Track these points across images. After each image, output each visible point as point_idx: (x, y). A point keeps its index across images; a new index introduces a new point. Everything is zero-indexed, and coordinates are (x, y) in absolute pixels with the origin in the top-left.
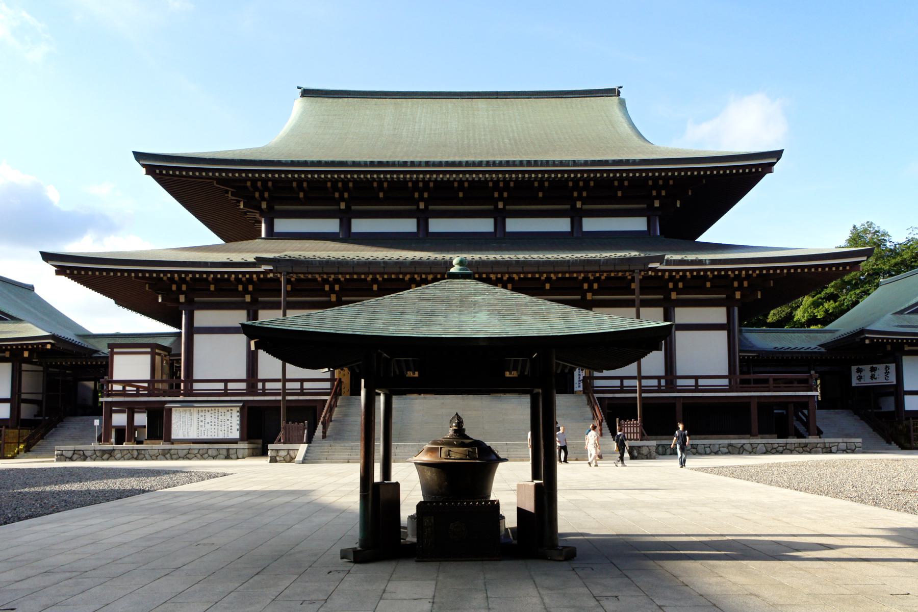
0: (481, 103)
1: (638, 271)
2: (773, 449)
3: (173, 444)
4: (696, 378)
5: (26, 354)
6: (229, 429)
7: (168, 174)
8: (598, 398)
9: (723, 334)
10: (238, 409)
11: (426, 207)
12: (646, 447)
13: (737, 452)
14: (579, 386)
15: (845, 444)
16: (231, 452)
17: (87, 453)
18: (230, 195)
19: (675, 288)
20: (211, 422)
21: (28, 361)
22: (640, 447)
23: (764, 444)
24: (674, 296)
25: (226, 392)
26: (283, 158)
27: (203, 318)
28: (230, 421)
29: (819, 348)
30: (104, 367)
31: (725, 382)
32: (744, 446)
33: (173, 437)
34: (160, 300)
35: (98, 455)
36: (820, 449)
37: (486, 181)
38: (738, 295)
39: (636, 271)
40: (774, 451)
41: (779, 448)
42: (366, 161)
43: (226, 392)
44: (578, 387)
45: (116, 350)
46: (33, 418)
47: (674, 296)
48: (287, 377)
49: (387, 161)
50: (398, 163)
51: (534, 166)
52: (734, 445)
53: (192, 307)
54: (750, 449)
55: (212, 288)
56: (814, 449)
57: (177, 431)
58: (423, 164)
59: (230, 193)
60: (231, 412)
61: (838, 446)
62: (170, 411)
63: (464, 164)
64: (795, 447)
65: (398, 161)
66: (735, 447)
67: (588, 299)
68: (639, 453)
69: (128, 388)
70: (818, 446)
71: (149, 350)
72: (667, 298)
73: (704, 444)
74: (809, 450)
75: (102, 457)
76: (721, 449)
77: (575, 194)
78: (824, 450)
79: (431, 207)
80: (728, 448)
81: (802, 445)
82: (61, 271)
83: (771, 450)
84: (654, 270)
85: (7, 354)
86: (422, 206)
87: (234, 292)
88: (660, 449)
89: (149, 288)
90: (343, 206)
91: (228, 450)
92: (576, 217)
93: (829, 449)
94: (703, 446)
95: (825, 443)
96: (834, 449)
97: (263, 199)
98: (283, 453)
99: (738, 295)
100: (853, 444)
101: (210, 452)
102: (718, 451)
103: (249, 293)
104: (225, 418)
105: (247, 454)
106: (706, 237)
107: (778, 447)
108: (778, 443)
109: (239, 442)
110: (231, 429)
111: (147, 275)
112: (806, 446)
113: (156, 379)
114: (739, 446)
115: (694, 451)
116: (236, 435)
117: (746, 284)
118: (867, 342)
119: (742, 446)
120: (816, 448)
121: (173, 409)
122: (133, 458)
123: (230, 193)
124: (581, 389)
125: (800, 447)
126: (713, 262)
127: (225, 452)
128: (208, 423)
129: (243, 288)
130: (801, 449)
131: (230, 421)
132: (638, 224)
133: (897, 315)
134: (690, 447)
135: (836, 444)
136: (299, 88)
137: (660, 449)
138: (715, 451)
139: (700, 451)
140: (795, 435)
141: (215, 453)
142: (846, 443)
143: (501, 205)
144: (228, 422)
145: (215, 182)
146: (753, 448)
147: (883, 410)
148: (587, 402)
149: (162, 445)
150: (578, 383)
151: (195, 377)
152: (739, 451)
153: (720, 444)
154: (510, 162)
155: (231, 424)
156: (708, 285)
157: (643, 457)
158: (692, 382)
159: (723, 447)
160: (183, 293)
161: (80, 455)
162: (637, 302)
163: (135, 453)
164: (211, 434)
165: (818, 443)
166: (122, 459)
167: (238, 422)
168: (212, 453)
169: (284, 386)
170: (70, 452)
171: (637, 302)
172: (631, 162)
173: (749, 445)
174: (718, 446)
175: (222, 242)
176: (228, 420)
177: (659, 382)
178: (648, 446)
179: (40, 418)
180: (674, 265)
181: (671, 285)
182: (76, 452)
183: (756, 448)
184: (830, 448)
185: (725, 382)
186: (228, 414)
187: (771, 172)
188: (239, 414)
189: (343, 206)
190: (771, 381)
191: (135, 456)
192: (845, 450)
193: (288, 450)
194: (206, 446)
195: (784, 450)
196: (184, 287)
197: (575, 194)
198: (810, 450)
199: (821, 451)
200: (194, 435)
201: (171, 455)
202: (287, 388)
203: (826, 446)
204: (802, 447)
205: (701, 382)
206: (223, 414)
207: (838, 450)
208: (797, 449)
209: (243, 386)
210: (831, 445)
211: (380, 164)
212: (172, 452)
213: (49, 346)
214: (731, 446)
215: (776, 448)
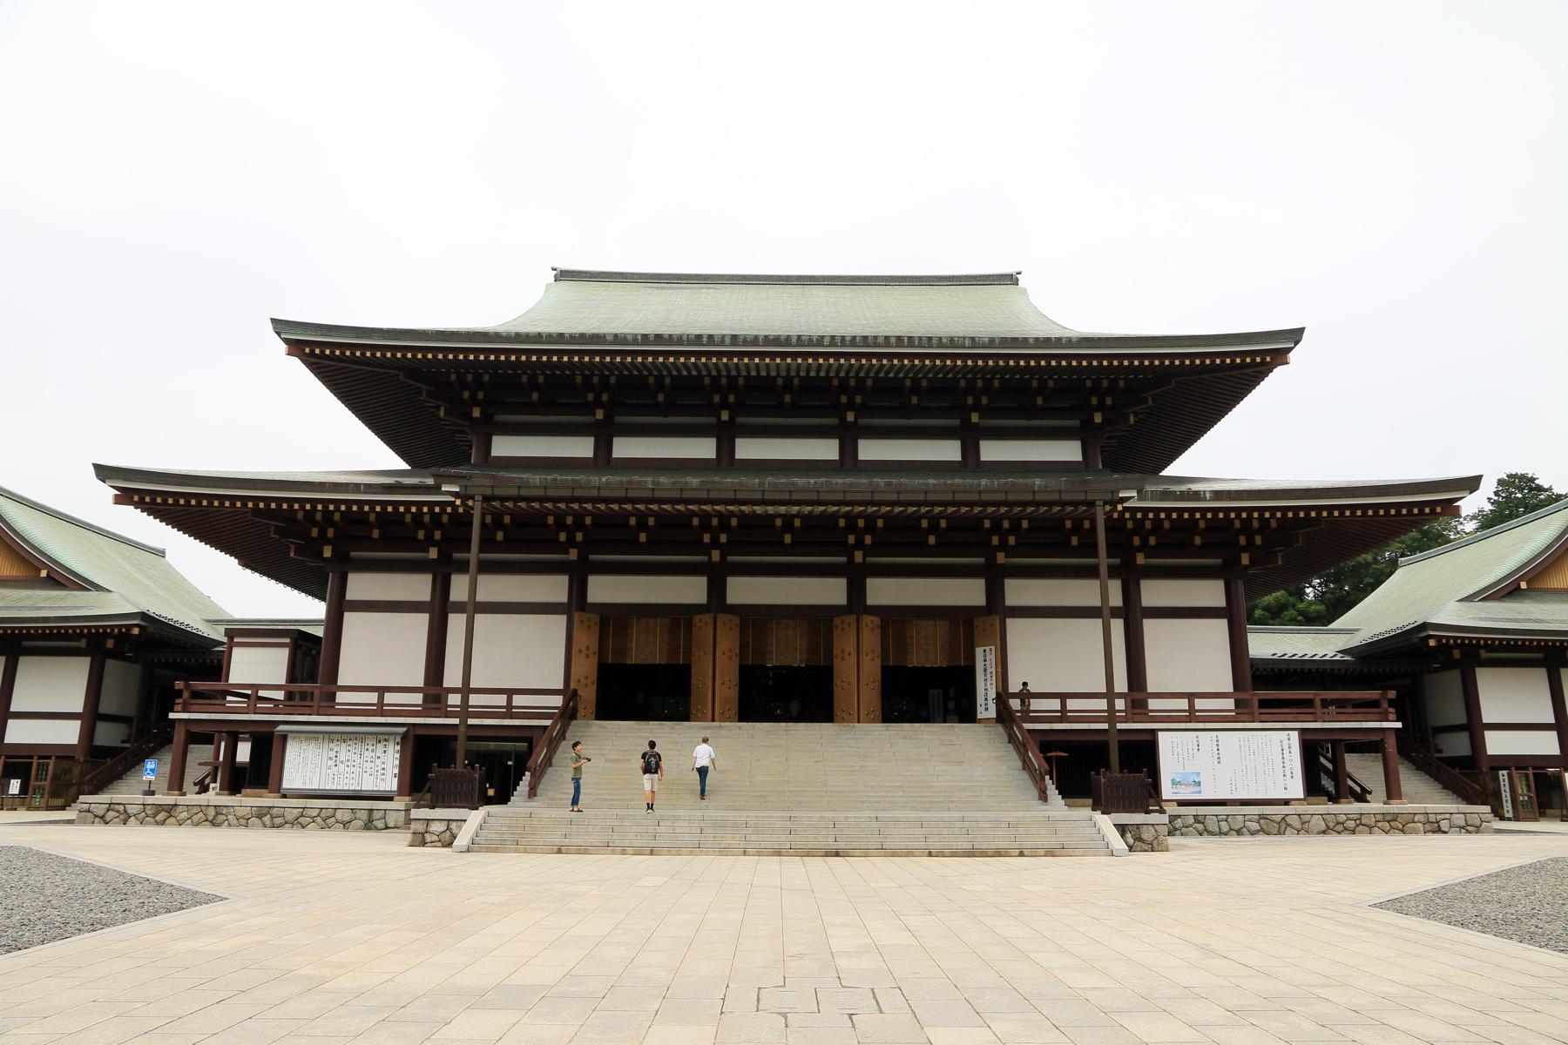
2: (1338, 823)
3: (284, 796)
5: (110, 644)
9: (1222, 625)
10: (398, 739)
11: (732, 418)
12: (1151, 828)
14: (987, 709)
15: (1462, 816)
16: (376, 815)
17: (131, 810)
19: (1144, 547)
20: (348, 760)
21: (116, 655)
22: (1138, 826)
23: (1321, 815)
24: (1141, 559)
25: (380, 709)
27: (360, 586)
32: (1287, 819)
33: (286, 784)
35: (149, 812)
36: (1420, 825)
39: (1097, 503)
40: (1340, 828)
42: (636, 335)
43: (380, 709)
44: (986, 707)
46: (120, 745)
47: (1141, 559)
48: (473, 685)
49: (670, 335)
50: (688, 338)
53: (345, 565)
54: (1298, 826)
55: (376, 534)
56: (1409, 825)
57: (294, 775)
58: (728, 340)
60: (385, 743)
63: (794, 340)
64: (1376, 821)
71: (288, 640)
75: (154, 818)
76: (1248, 824)
77: (970, 400)
78: (1428, 827)
81: (1388, 818)
83: (1335, 826)
85: (83, 643)
86: (725, 416)
87: (412, 544)
90: (600, 415)
91: (371, 810)
92: (970, 440)
93: (1436, 825)
94: (1215, 817)
95: (1427, 814)
96: (1444, 825)
97: (476, 402)
98: (437, 827)
101: (339, 814)
103: (434, 544)
105: (403, 820)
109: (396, 798)
110: (383, 774)
111: (262, 505)
113: (230, 682)
114: (1278, 818)
115: (1200, 827)
116: (390, 784)
117: (1258, 540)
118: (1432, 643)
121: (290, 735)
122: (207, 820)
124: (992, 713)
125: (1384, 821)
127: (364, 815)
128: (342, 762)
129: (426, 535)
133: (1465, 604)
135: (1448, 816)
136: (554, 269)
138: (1237, 827)
141: (347, 816)
143: (850, 417)
144: (378, 762)
145: (401, 374)
147: (1444, 755)
148: (1007, 739)
149: (267, 800)
150: (983, 704)
154: (870, 338)
156: (1198, 540)
160: (328, 542)
161: (118, 812)
163: (212, 812)
164: (346, 781)
165: (1415, 814)
166: (189, 821)
167: (397, 762)
168: (343, 817)
169: (465, 700)
170: (103, 805)
172: (1064, 342)
175: (407, 467)
176: (379, 758)
177: (1111, 705)
178: (1153, 825)
179: (128, 745)
180: (1152, 500)
181: (1136, 541)
184: (1437, 822)
185: (1229, 704)
186: (380, 747)
187: (1287, 363)
188: (398, 748)
189: (600, 415)
190: (1318, 703)
191: (210, 818)
192: (1463, 827)
193: (449, 820)
194: (333, 803)
195: (1358, 825)
196: (330, 533)
197: (970, 400)
199: (1422, 829)
200: (314, 784)
201: (272, 817)
202: (514, 705)
203: (1430, 820)
204: (1389, 822)
205: (1200, 704)
207: (1451, 827)
208: (1380, 824)
209: (418, 698)
210: (1439, 817)
211: (659, 338)
212: (274, 811)
213: (136, 631)
214: (1265, 818)
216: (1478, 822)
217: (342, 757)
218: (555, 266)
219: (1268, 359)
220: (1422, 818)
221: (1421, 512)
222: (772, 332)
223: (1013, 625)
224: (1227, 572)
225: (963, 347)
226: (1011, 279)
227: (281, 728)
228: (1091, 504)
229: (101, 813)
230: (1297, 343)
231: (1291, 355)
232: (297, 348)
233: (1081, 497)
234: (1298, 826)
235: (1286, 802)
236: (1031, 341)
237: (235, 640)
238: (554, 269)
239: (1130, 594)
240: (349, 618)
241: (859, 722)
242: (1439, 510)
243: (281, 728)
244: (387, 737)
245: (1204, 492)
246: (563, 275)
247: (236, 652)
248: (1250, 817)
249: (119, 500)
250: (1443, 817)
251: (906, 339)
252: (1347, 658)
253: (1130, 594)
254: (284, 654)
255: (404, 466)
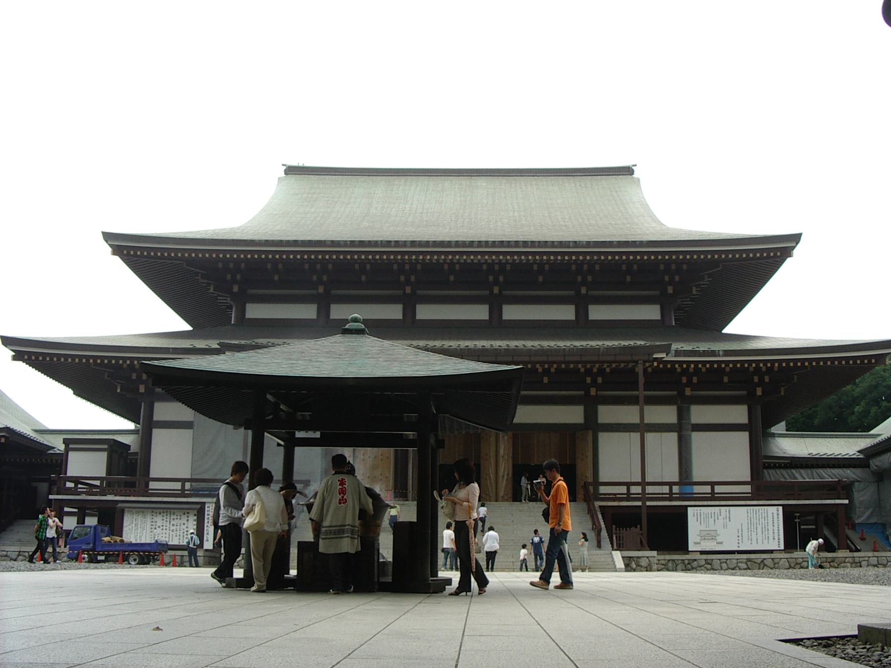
0: (482, 182)
1: (642, 362)
2: (797, 564)
4: (713, 484)
6: (185, 534)
7: (142, 255)
8: (600, 507)
9: (744, 436)
10: (196, 512)
12: (646, 558)
13: (757, 568)
15: (876, 559)
18: (199, 278)
22: (638, 557)
23: (787, 558)
26: (256, 238)
28: (186, 526)
29: (858, 454)
30: (61, 462)
31: (747, 489)
32: (765, 561)
34: (119, 391)
36: (849, 564)
37: (480, 263)
38: (759, 392)
39: (639, 362)
41: (804, 563)
45: (71, 446)
47: (688, 392)
50: (381, 243)
51: (530, 247)
52: (753, 560)
53: (151, 399)
54: (772, 566)
57: (129, 534)
58: (408, 244)
59: (200, 275)
60: (188, 515)
61: (868, 561)
62: (122, 512)
65: (382, 241)
66: (754, 562)
67: (592, 394)
68: (638, 565)
69: (80, 486)
70: (847, 561)
71: (106, 447)
72: (681, 394)
73: (720, 560)
74: (836, 565)
76: (740, 564)
79: (419, 292)
80: (746, 564)
81: (829, 560)
82: (18, 356)
83: (795, 566)
84: (659, 360)
88: (670, 564)
89: (108, 377)
90: (321, 290)
93: (859, 564)
94: (719, 561)
95: (854, 557)
99: (759, 392)
100: (885, 558)
102: (735, 567)
104: (180, 521)
106: (729, 329)
107: (803, 561)
108: (802, 558)
112: (833, 561)
114: (759, 561)
115: (709, 566)
117: (767, 379)
119: (762, 561)
120: (845, 562)
121: (126, 510)
123: (200, 275)
125: (826, 562)
126: (727, 353)
127: (178, 559)
130: (828, 564)
131: (186, 526)
132: (651, 312)
134: (704, 563)
135: (866, 559)
136: (283, 165)
137: (670, 564)
139: (715, 567)
140: (826, 551)
142: (877, 557)
143: (496, 290)
144: (184, 527)
146: (775, 564)
151: (151, 476)
152: (759, 566)
153: (737, 559)
155: (187, 529)
156: (726, 379)
157: (642, 569)
158: (708, 489)
159: (741, 562)
160: (142, 382)
161: (25, 556)
162: (641, 400)
165: (846, 558)
171: (641, 400)
173: (770, 560)
174: (735, 561)
175: (188, 328)
176: (184, 524)
178: (648, 557)
180: (684, 356)
182: (21, 553)
183: (778, 563)
185: (747, 489)
186: (184, 518)
197: (579, 279)
198: (838, 565)
199: (850, 566)
203: (855, 561)
204: (829, 562)
205: (718, 489)
206: (179, 517)
210: (861, 559)
214: (750, 561)
215: (800, 564)
216: (885, 562)
217: (159, 523)
218: (284, 163)
219: (779, 254)
220: (850, 560)
221: (870, 362)
222: (440, 239)
223: (603, 437)
224: (748, 400)
225: (569, 247)
226: (628, 171)
227: (120, 505)
228: (637, 362)
229: (14, 557)
230: (797, 243)
231: (795, 252)
232: (118, 251)
233: (629, 358)
234: (772, 566)
235: (771, 552)
236: (615, 243)
237: (71, 446)
238: (283, 165)
239: (682, 414)
240: (156, 432)
241: (496, 501)
242: (873, 361)
243: (120, 505)
244: (189, 511)
245: (719, 351)
246: (291, 171)
247: (71, 454)
248: (740, 560)
249: (15, 358)
250: (863, 559)
251: (529, 243)
252: (861, 456)
253: (682, 414)
254: (103, 457)
255: (186, 327)
